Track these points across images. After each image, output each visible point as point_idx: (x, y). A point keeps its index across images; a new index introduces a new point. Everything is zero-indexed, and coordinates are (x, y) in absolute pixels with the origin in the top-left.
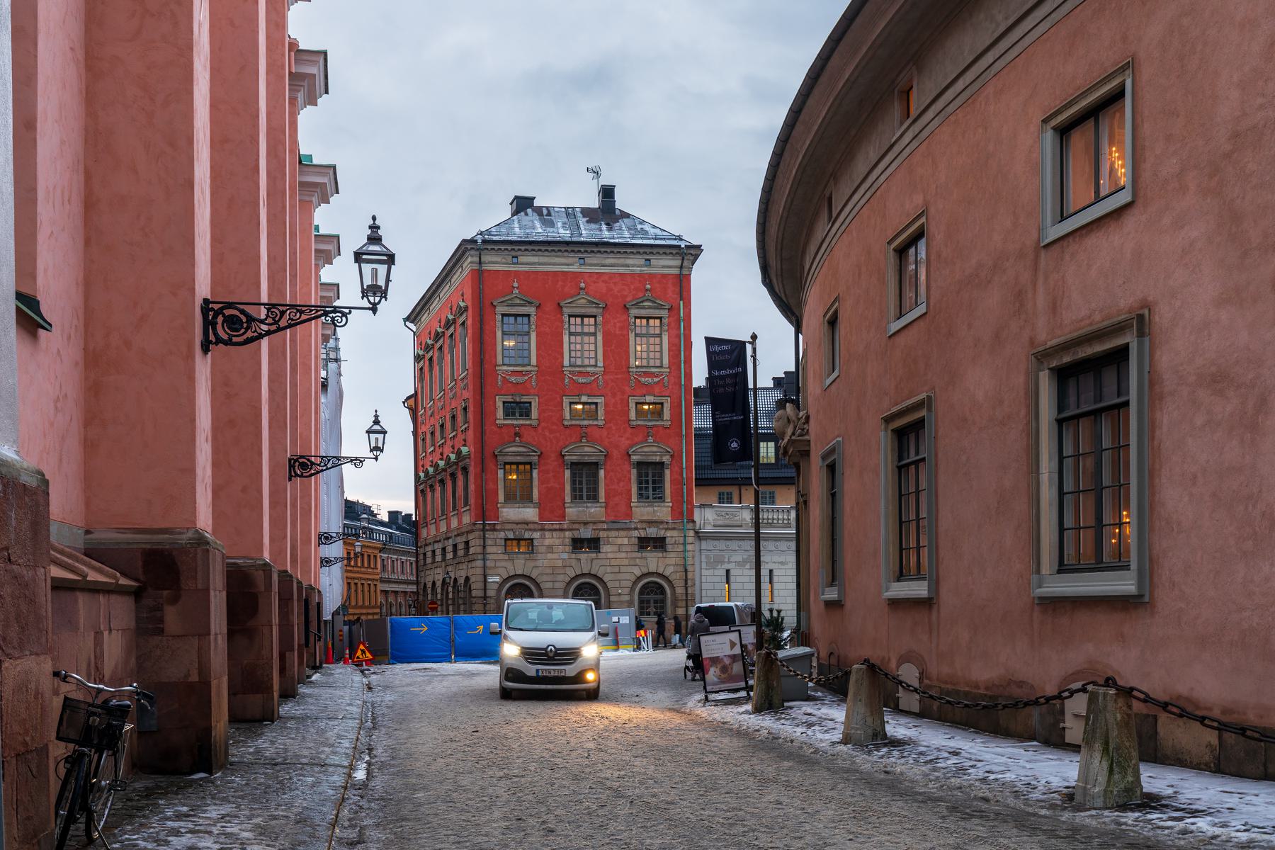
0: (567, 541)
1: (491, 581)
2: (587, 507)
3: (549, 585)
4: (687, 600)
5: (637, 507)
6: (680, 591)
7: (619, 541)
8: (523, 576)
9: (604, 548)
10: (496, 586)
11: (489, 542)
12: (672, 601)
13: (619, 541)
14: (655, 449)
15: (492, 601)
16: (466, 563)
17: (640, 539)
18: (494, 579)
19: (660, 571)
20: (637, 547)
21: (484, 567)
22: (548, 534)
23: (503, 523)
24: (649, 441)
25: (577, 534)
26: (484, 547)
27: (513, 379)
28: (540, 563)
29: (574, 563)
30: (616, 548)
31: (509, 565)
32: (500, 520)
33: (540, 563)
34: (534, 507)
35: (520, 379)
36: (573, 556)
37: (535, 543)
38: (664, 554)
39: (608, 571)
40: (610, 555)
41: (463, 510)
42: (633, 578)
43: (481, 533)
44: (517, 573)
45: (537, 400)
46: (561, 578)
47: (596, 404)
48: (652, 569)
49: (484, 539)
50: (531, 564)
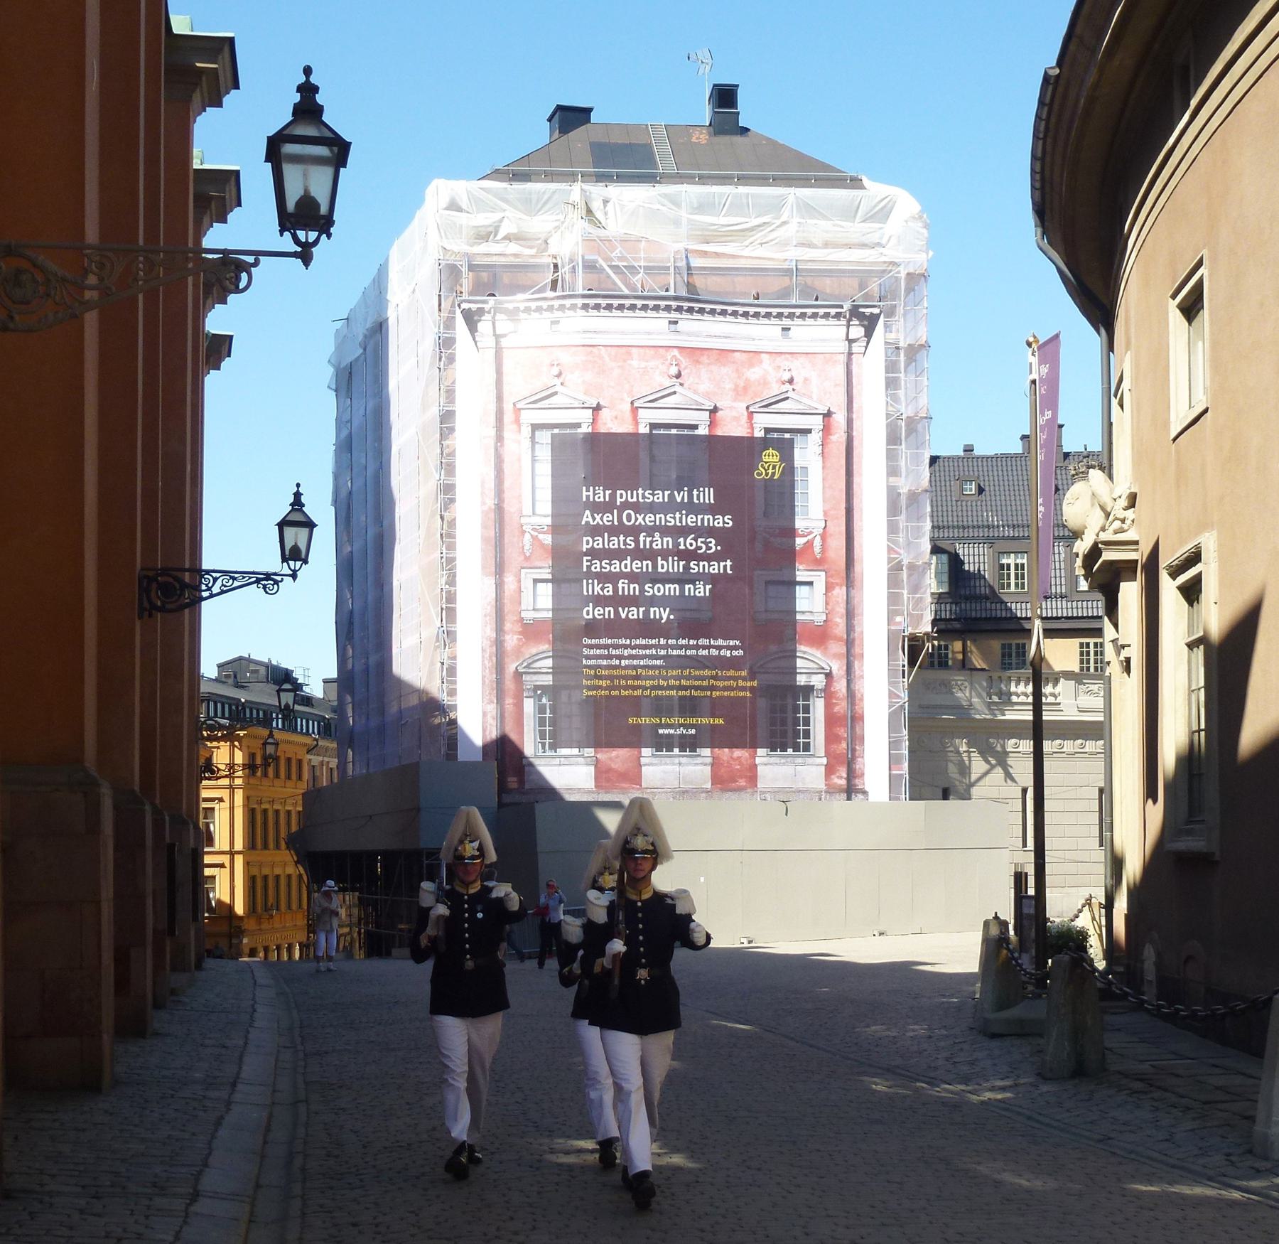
34: (588, 764)
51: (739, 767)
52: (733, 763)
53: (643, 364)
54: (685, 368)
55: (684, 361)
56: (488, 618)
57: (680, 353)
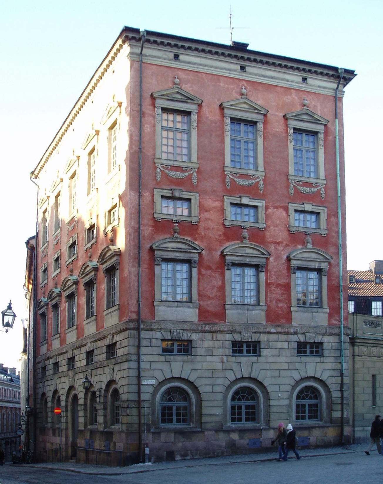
0: (228, 344)
1: (146, 383)
2: (248, 309)
3: (208, 389)
4: (342, 404)
5: (296, 311)
6: (336, 394)
7: (279, 345)
8: (180, 379)
9: (264, 352)
10: (151, 390)
11: (144, 342)
12: (327, 405)
13: (279, 345)
14: (314, 256)
15: (147, 405)
16: (112, 367)
17: (299, 344)
18: (148, 382)
19: (318, 375)
20: (296, 351)
21: (139, 369)
22: (209, 336)
23: (159, 322)
24: (308, 247)
25: (238, 338)
26: (139, 347)
27: (173, 173)
28: (198, 366)
29: (235, 366)
30: (276, 352)
31: (165, 367)
32: (156, 319)
33: (198, 366)
34: (194, 307)
35: (179, 175)
36: (233, 359)
37: (194, 345)
38: (322, 358)
39: (269, 375)
40: (271, 359)
41: (105, 313)
42: (293, 382)
43: (135, 332)
44: (174, 376)
45: (198, 198)
46: (220, 381)
47: (256, 207)
48: (311, 374)
49: (139, 338)
50: (188, 367)
51: (281, 312)
52: (278, 310)
53: (226, 86)
54: (250, 91)
55: (248, 88)
56: (133, 216)
57: (246, 83)
